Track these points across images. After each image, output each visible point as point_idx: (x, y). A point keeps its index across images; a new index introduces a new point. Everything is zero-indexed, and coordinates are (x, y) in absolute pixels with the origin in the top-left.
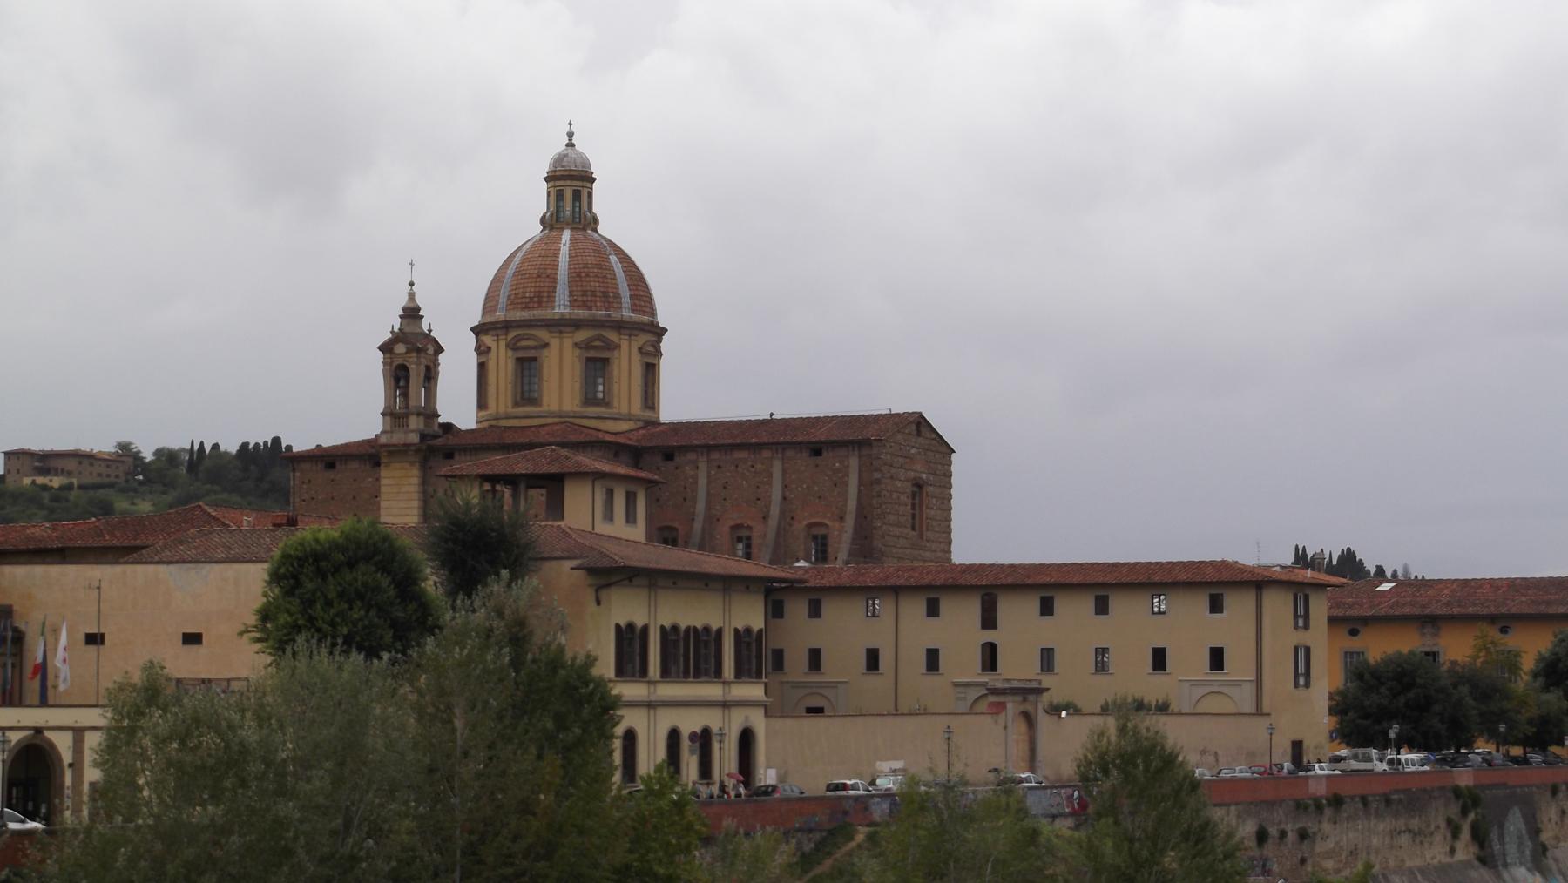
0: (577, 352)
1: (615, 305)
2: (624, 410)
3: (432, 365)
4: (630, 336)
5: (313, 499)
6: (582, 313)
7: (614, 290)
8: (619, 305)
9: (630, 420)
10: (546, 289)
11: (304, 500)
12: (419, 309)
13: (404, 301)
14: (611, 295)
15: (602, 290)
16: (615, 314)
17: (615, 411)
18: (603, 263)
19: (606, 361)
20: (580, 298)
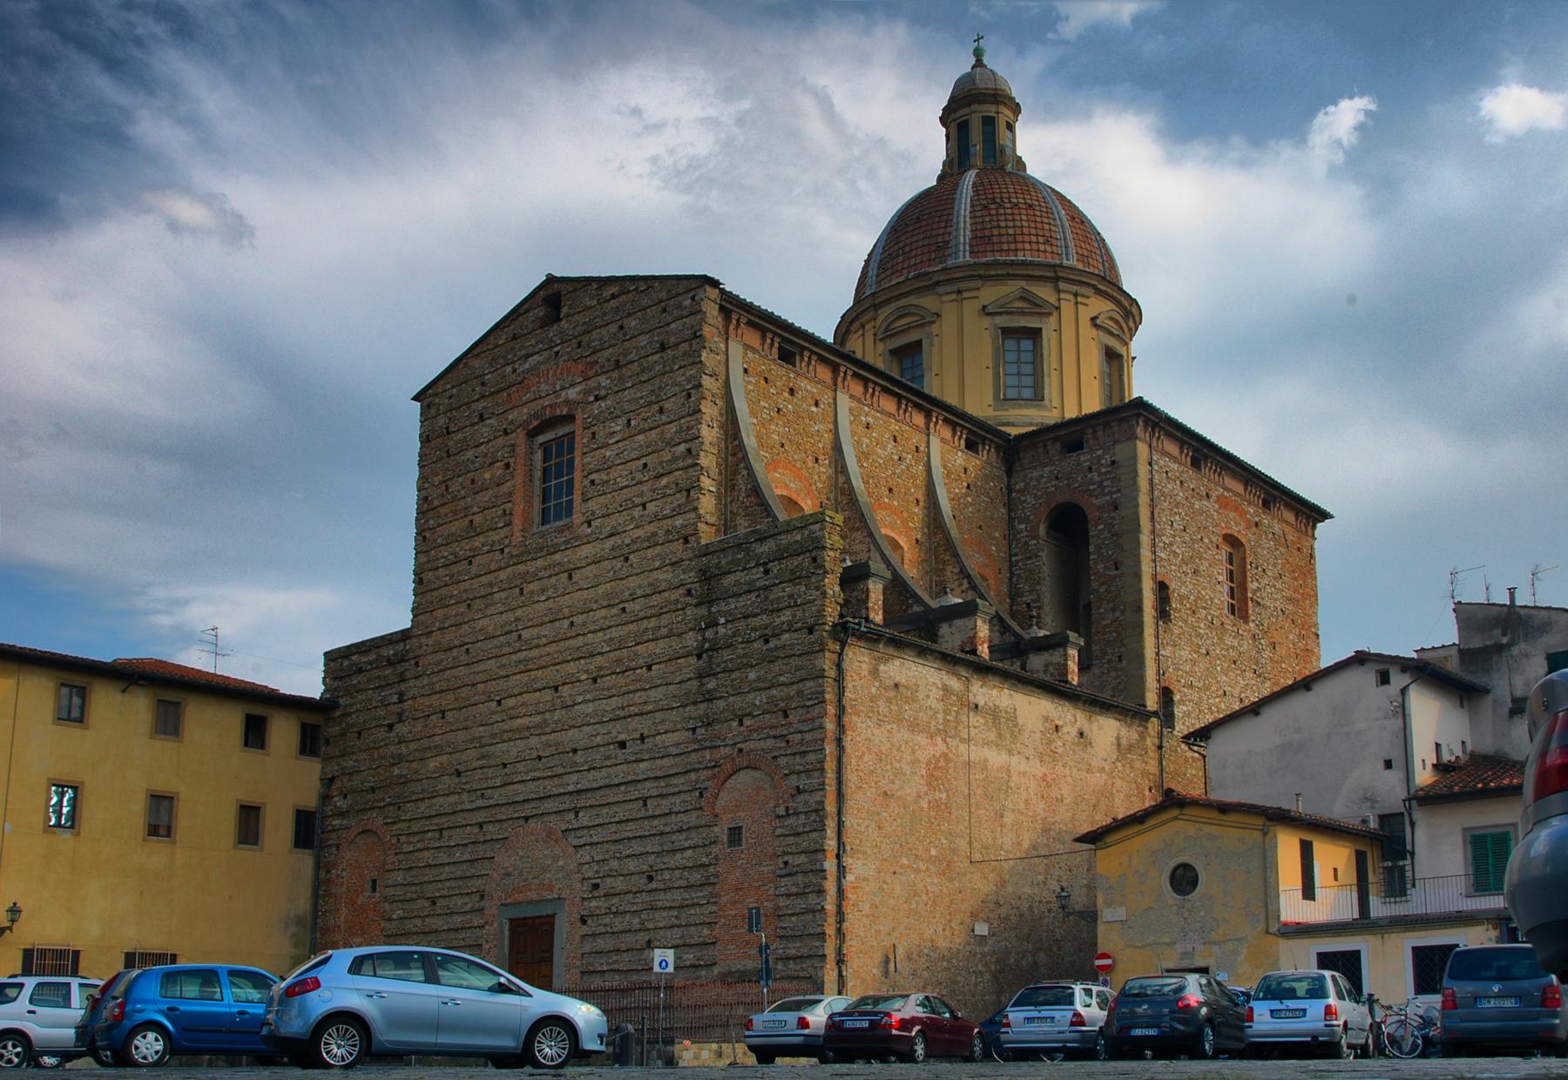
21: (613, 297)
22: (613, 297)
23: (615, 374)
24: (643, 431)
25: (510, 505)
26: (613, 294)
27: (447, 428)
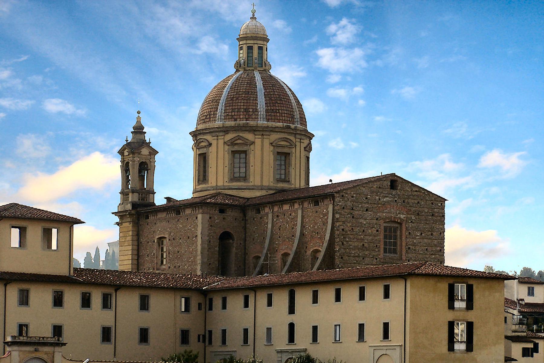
0: (227, 147)
1: (254, 117)
2: (258, 183)
3: (148, 161)
4: (263, 135)
6: (231, 123)
7: (254, 107)
8: (256, 117)
9: (262, 189)
10: (213, 110)
12: (143, 128)
13: (134, 123)
14: (251, 110)
15: (245, 107)
16: (252, 123)
17: (251, 184)
18: (250, 91)
19: (245, 152)
20: (230, 114)
21: (416, 191)
22: (416, 191)
23: (417, 217)
24: (427, 238)
25: (379, 244)
26: (416, 191)
27: (352, 208)
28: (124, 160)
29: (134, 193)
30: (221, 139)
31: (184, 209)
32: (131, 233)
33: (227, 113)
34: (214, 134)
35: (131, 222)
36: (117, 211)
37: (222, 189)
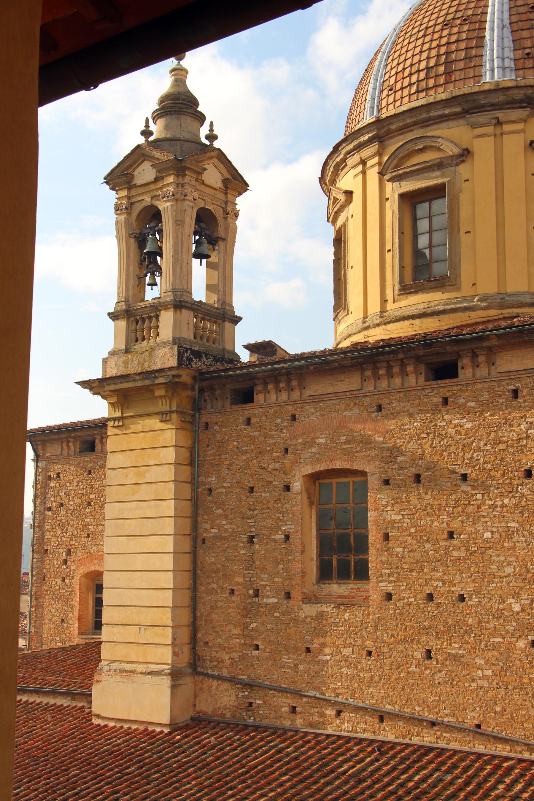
3: (219, 214)
5: (62, 505)
11: (50, 509)
28: (132, 204)
29: (184, 311)
30: (512, 132)
31: (490, 351)
32: (170, 455)
33: (525, 48)
34: (482, 118)
35: (171, 412)
36: (100, 376)
37: (522, 305)
